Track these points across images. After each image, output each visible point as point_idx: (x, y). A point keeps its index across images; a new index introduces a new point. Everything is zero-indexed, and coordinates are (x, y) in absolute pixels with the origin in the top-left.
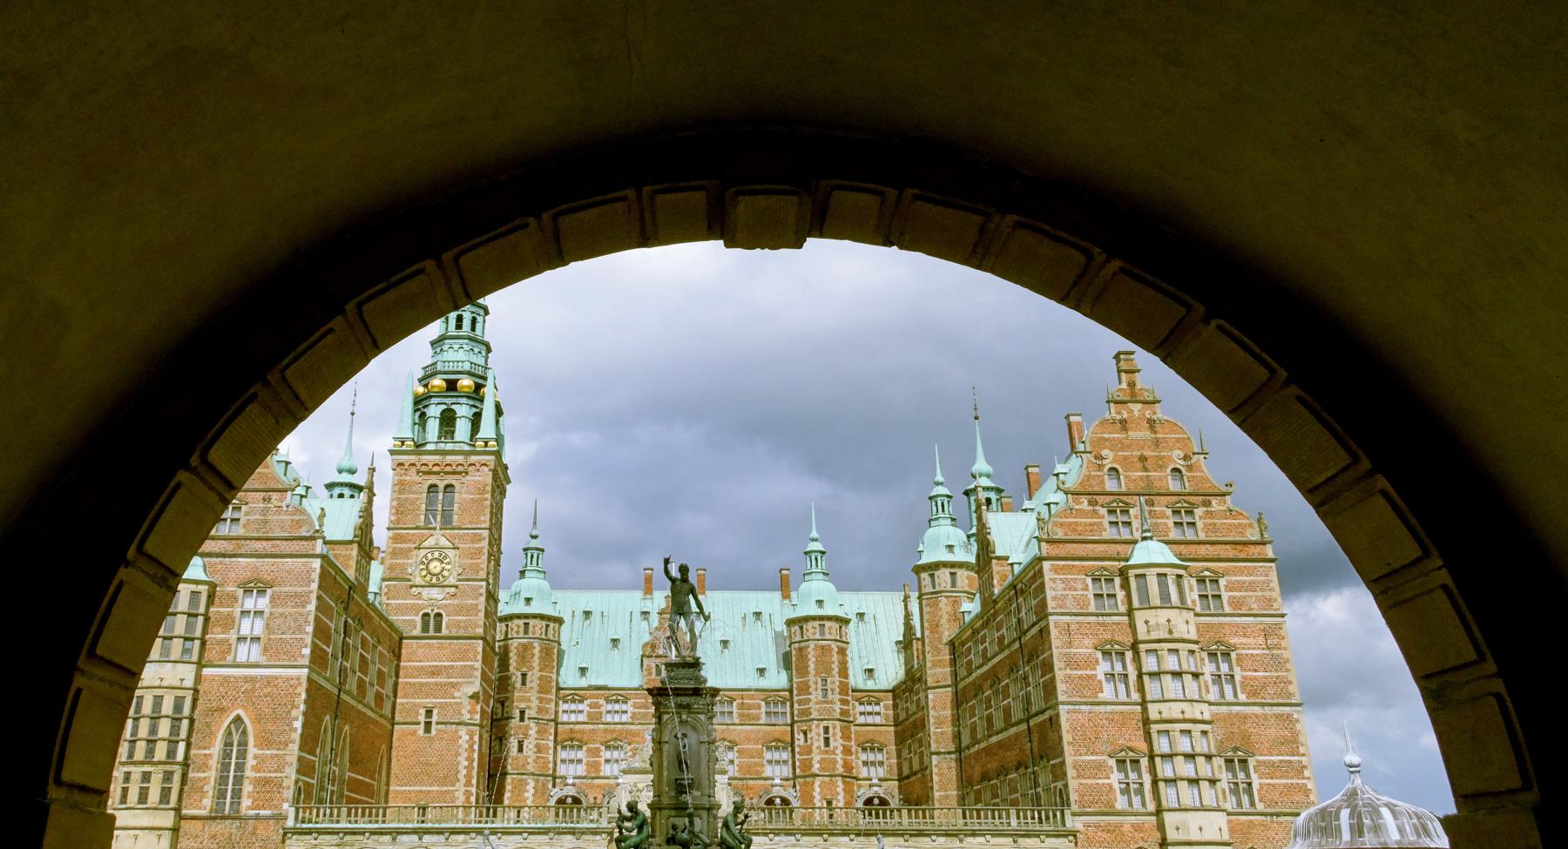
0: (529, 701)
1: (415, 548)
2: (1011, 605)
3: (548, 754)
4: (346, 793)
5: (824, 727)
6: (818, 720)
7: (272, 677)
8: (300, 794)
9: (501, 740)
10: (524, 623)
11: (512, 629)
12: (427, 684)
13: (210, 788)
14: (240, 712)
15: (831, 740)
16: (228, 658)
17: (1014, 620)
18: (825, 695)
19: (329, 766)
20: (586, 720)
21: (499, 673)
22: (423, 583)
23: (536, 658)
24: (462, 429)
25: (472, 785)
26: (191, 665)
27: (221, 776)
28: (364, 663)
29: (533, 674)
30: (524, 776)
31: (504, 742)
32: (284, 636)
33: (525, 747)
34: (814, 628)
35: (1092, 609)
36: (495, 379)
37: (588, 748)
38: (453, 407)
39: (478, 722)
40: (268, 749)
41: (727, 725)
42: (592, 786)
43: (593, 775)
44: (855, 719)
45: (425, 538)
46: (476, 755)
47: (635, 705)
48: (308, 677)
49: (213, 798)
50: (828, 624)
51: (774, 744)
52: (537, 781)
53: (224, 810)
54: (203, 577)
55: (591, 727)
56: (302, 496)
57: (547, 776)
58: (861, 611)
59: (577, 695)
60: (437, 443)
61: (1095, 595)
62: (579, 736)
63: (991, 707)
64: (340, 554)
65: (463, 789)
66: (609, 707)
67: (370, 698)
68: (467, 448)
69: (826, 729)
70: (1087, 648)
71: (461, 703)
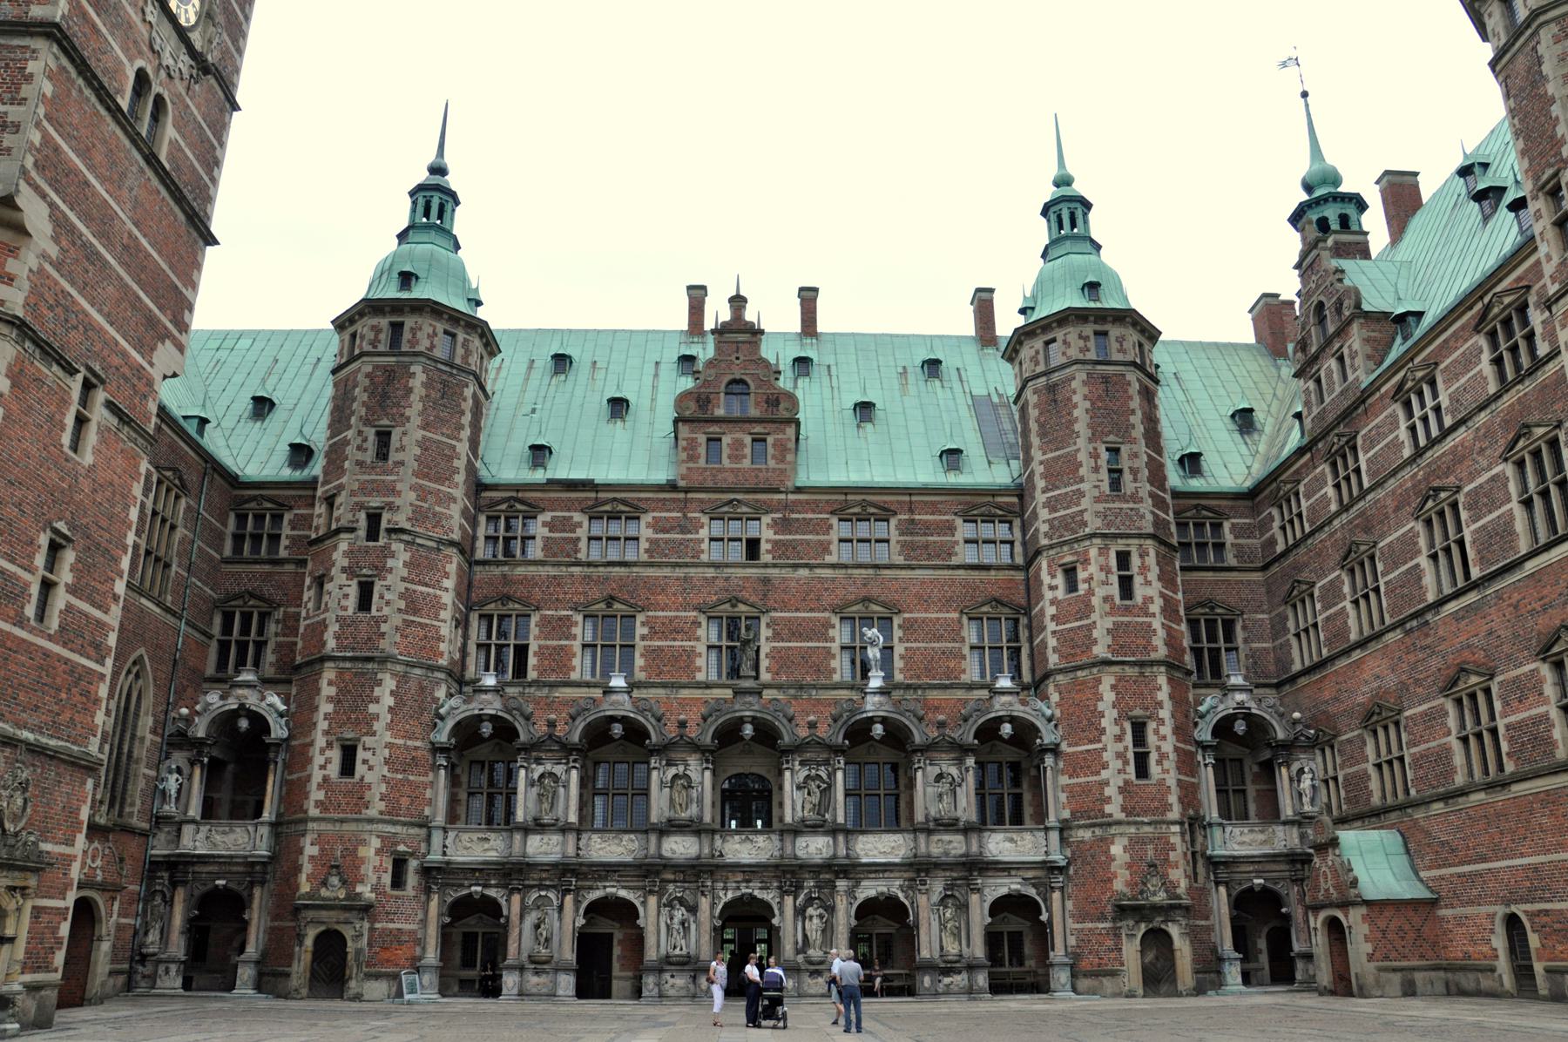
0: (393, 491)
3: (436, 618)
5: (1119, 554)
6: (1104, 536)
9: (321, 586)
10: (393, 325)
11: (362, 337)
15: (1138, 580)
18: (1116, 484)
21: (331, 437)
23: (415, 397)
29: (404, 433)
30: (370, 666)
31: (328, 587)
34: (1086, 339)
37: (544, 617)
41: (876, 567)
42: (550, 705)
43: (553, 678)
47: (658, 526)
50: (1115, 331)
51: (985, 609)
52: (403, 679)
55: (552, 571)
57: (439, 669)
62: (520, 591)
66: (598, 528)
69: (1123, 559)
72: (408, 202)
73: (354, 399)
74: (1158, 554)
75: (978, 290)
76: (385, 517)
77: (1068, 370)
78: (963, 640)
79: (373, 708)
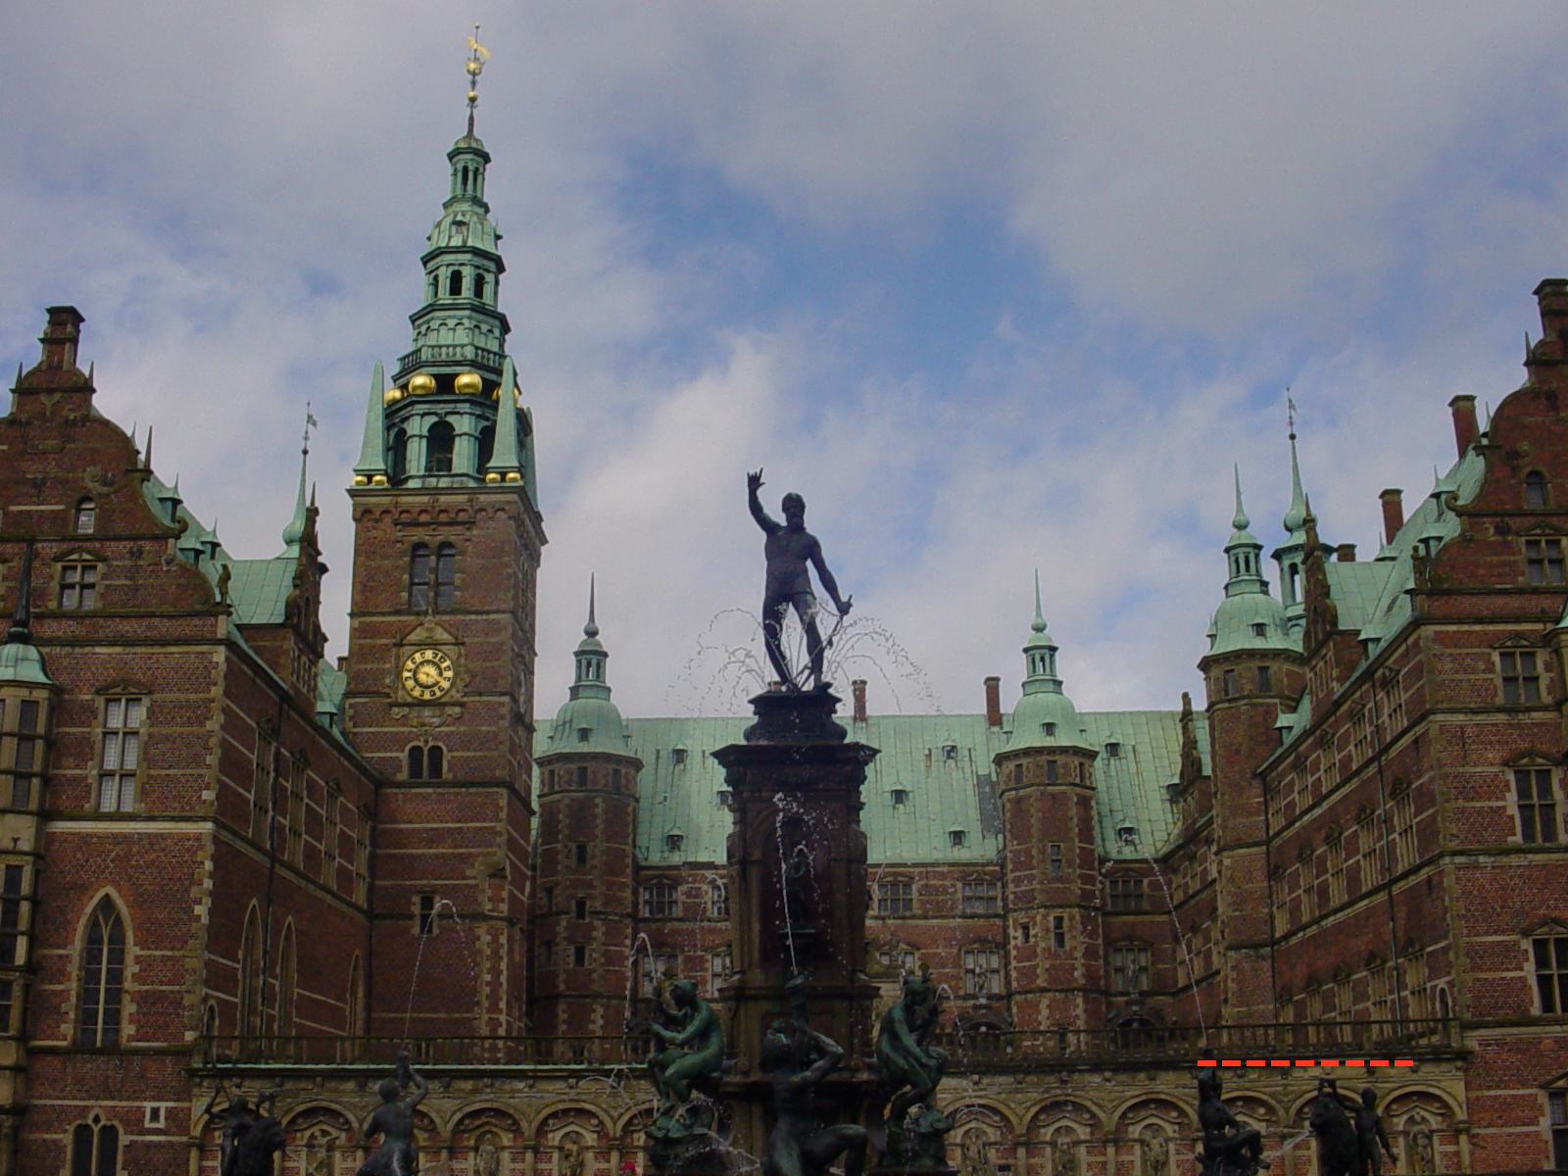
1: (395, 645)
2: (1364, 706)
4: (295, 1019)
5: (1055, 918)
7: (156, 835)
8: (212, 1018)
10: (579, 768)
12: (423, 854)
13: (70, 1006)
14: (109, 890)
16: (87, 806)
17: (1369, 730)
19: (261, 977)
20: (681, 914)
21: (543, 844)
22: (409, 700)
23: (598, 821)
24: (463, 455)
25: (500, 1011)
26: (29, 817)
27: (86, 990)
28: (314, 823)
29: (595, 846)
30: (587, 1000)
31: (554, 949)
32: (172, 772)
33: (587, 953)
34: (1042, 767)
35: (1500, 700)
36: (515, 374)
38: (450, 419)
39: (505, 914)
40: (156, 949)
44: (1104, 905)
45: (409, 629)
46: (503, 966)
48: (215, 836)
49: (76, 1022)
50: (1060, 759)
51: (976, 946)
52: (607, 1007)
53: (95, 1041)
54: (42, 678)
56: (198, 553)
58: (1113, 741)
59: (666, 877)
60: (424, 476)
61: (1506, 680)
63: (1327, 872)
64: (265, 647)
65: (486, 1017)
67: (329, 876)
68: (472, 484)
70: (1492, 764)
71: (477, 885)
72: (573, 659)
73: (559, 822)
74: (1082, 916)
75: (988, 680)
76: (588, 904)
77: (1028, 790)
78: (960, 967)
79: (591, 1027)
